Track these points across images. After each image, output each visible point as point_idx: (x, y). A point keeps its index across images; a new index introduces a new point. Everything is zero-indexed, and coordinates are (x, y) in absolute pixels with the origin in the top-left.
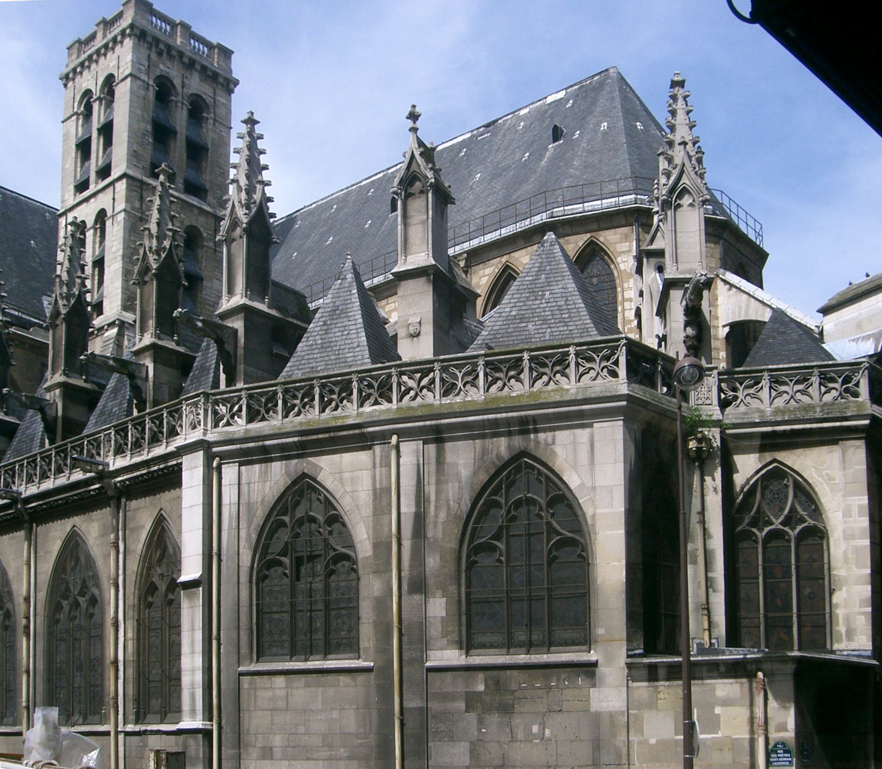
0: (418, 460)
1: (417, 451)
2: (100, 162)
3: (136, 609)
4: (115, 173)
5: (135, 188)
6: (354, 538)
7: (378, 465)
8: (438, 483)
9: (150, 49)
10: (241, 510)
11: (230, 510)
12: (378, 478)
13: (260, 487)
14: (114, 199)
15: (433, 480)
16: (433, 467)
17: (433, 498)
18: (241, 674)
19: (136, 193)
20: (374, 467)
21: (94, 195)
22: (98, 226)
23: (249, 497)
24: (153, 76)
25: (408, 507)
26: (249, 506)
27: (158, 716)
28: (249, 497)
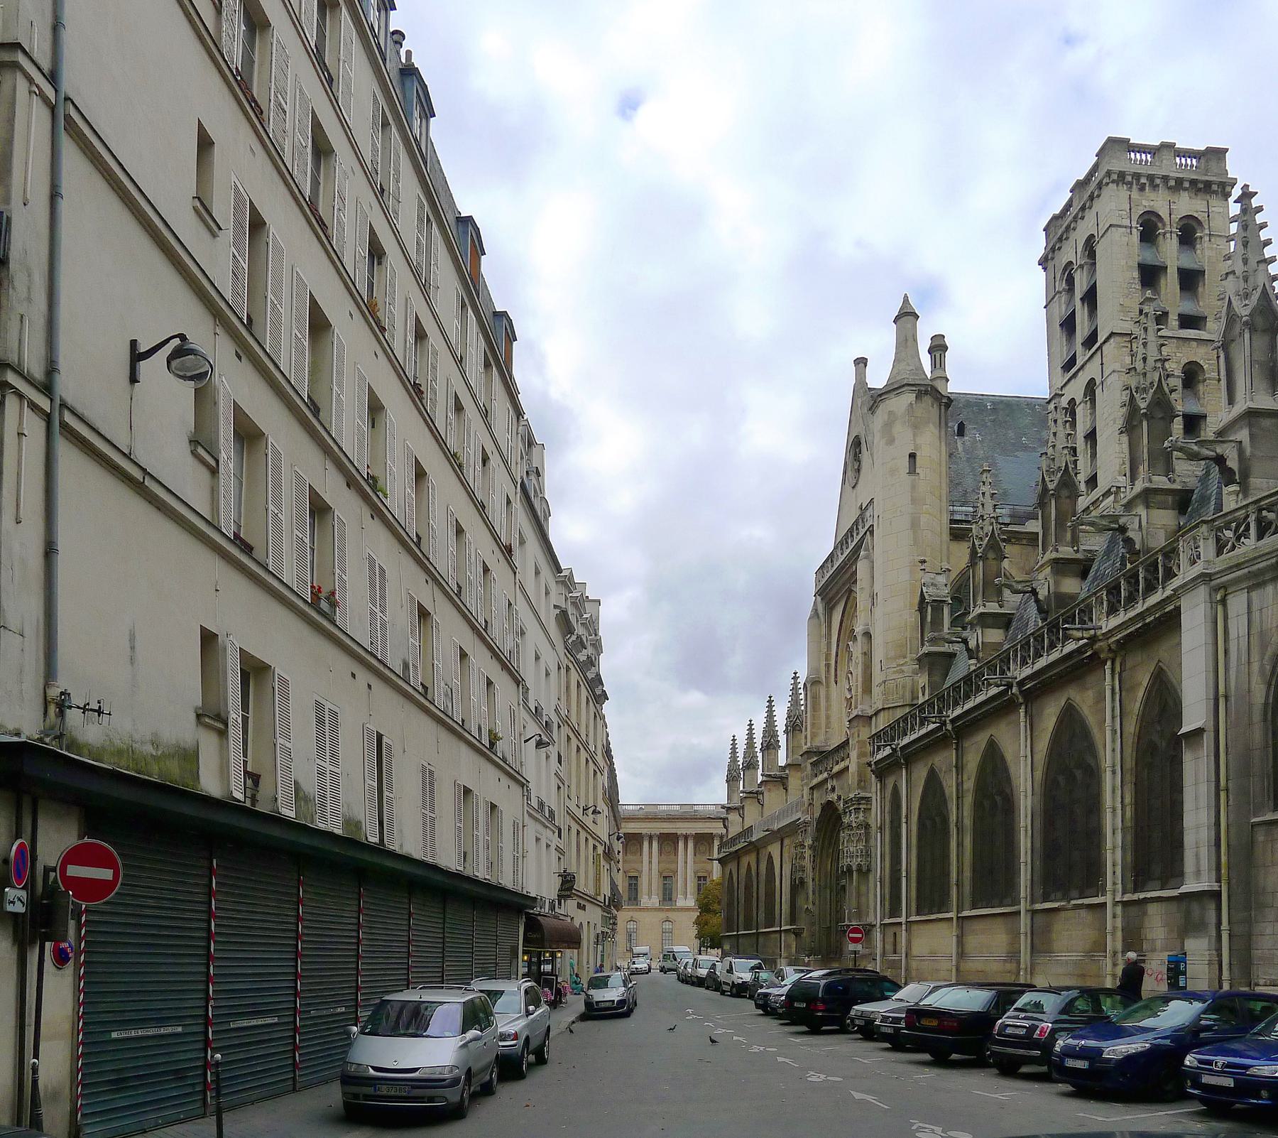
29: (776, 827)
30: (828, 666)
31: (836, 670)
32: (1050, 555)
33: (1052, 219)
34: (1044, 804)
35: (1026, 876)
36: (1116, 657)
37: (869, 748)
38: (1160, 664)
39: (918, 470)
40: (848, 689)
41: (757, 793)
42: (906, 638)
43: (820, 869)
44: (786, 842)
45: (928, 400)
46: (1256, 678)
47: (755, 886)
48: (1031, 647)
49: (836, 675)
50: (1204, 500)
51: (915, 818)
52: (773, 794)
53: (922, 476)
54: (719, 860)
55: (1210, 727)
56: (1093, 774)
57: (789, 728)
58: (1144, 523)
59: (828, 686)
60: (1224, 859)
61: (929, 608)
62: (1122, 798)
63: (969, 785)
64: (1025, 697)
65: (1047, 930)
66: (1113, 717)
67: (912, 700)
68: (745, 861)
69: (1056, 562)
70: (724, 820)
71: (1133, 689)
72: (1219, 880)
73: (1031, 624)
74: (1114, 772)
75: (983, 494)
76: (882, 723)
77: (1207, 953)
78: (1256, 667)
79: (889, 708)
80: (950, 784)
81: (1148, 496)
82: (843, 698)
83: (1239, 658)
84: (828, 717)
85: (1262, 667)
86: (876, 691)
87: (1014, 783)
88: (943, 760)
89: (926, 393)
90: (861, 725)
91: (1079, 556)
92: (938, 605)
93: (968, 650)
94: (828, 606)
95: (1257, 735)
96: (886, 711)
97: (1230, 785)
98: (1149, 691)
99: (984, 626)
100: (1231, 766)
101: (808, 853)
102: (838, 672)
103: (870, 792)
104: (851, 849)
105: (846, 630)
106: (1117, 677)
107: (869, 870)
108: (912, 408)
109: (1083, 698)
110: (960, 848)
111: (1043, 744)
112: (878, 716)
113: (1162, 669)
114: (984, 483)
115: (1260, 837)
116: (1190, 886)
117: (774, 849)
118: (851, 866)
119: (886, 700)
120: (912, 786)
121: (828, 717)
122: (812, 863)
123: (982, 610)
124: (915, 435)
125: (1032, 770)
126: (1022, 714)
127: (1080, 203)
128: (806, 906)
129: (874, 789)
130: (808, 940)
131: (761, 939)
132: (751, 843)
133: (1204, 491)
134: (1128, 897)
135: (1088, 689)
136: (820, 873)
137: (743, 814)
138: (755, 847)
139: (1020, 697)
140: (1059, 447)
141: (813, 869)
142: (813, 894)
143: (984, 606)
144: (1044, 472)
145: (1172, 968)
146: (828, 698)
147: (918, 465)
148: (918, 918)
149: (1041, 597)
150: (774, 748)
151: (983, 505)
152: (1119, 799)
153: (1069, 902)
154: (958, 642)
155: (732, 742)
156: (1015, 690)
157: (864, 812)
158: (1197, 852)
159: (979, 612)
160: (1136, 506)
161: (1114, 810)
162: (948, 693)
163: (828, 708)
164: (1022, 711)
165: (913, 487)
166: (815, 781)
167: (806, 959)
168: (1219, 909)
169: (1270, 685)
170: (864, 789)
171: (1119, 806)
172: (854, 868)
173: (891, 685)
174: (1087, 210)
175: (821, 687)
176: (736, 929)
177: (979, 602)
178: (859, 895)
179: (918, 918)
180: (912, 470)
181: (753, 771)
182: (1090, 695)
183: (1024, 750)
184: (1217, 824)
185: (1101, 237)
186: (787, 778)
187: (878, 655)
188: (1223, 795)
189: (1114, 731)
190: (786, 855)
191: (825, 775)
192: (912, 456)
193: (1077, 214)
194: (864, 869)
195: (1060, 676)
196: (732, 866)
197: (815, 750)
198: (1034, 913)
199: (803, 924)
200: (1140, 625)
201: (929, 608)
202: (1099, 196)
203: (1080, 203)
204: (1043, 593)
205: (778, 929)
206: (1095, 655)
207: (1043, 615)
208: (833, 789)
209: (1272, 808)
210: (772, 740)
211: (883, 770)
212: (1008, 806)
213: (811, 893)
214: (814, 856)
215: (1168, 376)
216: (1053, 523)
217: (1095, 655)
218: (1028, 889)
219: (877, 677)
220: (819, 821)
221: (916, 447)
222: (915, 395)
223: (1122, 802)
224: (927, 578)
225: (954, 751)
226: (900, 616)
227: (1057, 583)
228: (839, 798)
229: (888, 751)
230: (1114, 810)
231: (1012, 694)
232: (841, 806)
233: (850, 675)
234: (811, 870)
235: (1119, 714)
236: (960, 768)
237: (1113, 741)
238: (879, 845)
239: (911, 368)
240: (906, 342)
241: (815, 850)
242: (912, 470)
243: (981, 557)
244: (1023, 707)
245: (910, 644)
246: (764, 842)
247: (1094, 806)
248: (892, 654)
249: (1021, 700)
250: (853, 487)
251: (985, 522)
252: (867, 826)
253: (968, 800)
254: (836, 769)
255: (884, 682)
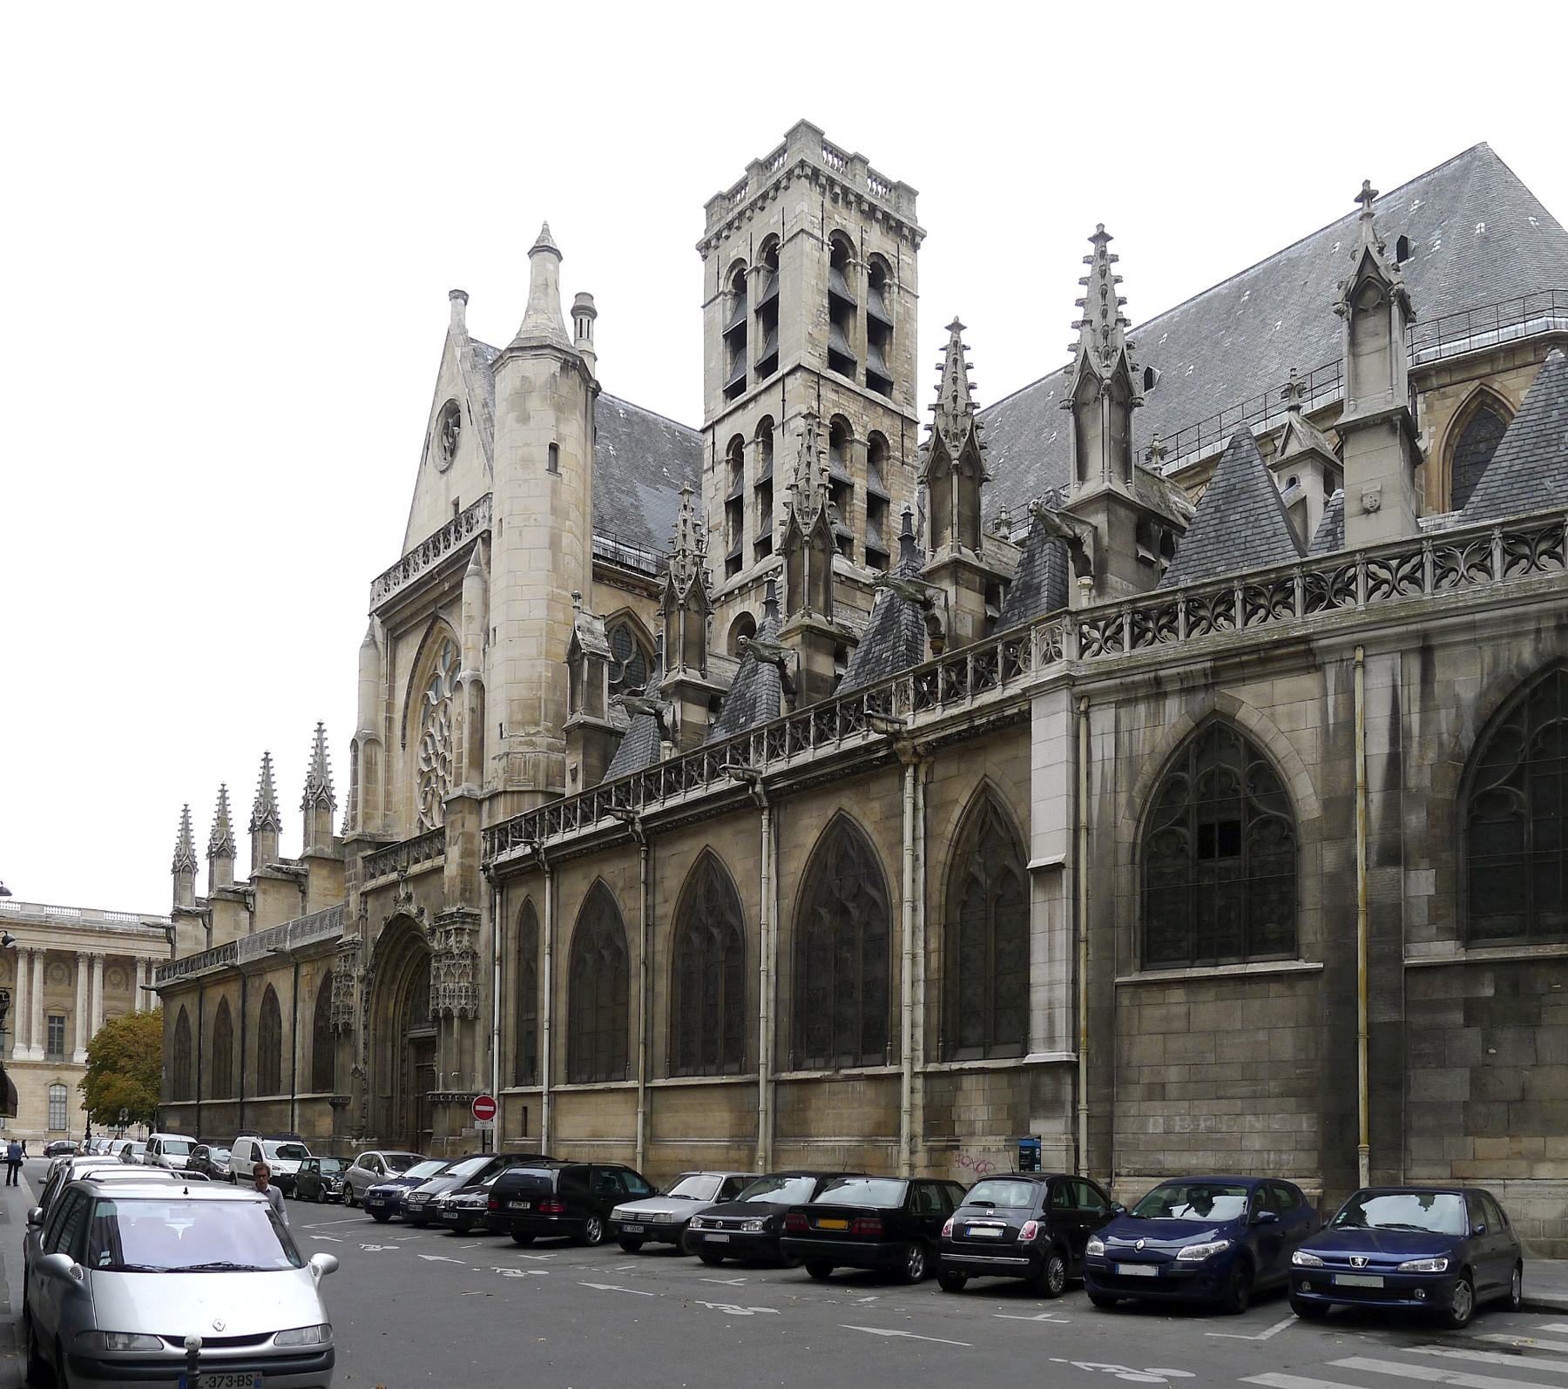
0: (1394, 680)
1: (1393, 669)
2: (760, 354)
3: (943, 911)
4: (784, 367)
5: (812, 384)
6: (1292, 794)
7: (1331, 691)
8: (1424, 710)
9: (823, 194)
10: (1119, 767)
11: (1103, 768)
12: (1331, 710)
13: (1148, 734)
14: (784, 400)
15: (1416, 708)
16: (1416, 689)
17: (1416, 730)
18: (1118, 986)
19: (812, 391)
20: (1325, 695)
21: (754, 398)
22: (760, 439)
23: (1131, 751)
24: (827, 232)
25: (1379, 746)
26: (1131, 761)
27: (981, 1049)
28: (1131, 751)
29: (288, 946)
30: (390, 720)
31: (404, 728)
32: (798, 619)
33: (716, 198)
34: (797, 943)
35: (767, 1036)
36: (920, 762)
37: (484, 846)
38: (987, 779)
39: (560, 470)
40: (424, 759)
41: (245, 894)
42: (540, 698)
43: (376, 1012)
44: (304, 970)
45: (575, 374)
46: (1122, 811)
47: (237, 1033)
48: (777, 738)
49: (404, 736)
50: (1030, 589)
51: (565, 949)
52: (270, 899)
53: (566, 477)
54: (160, 991)
55: (1069, 864)
56: (881, 913)
57: (311, 803)
58: (952, 601)
59: (389, 750)
60: (1083, 1023)
61: (586, 663)
62: (925, 942)
63: (667, 909)
64: (770, 800)
65: (802, 1106)
66: (914, 839)
67: (547, 785)
68: (215, 995)
69: (808, 630)
70: (168, 929)
71: (944, 806)
72: (1075, 1049)
73: (762, 707)
74: (914, 909)
75: (685, 521)
76: (502, 813)
77: (1063, 1137)
78: (1123, 798)
79: (513, 792)
80: (632, 907)
81: (955, 569)
82: (415, 772)
83: (1103, 786)
84: (388, 794)
85: (1130, 801)
86: (490, 765)
87: (748, 912)
88: (618, 873)
89: (574, 366)
90: (466, 811)
91: (833, 629)
92: (597, 659)
93: (661, 726)
94: (391, 636)
95: (1125, 879)
96: (509, 796)
97: (1090, 936)
98: (968, 813)
99: (684, 699)
100: (1091, 911)
101: (357, 989)
102: (408, 733)
103: (478, 908)
104: (448, 988)
105: (423, 672)
106: (920, 789)
107: (476, 1018)
108: (556, 381)
109: (866, 813)
110: (650, 993)
111: (797, 864)
112: (495, 802)
113: (989, 786)
114: (685, 507)
115: (1125, 1000)
116: (1038, 1056)
117: (282, 983)
118: (450, 1010)
119: (509, 780)
120: (560, 904)
121: (388, 794)
122: (364, 1004)
123: (681, 676)
124: (558, 420)
125: (777, 896)
126: (765, 823)
127: (759, 188)
128: (354, 1066)
129: (485, 903)
130: (357, 1114)
131: (249, 1112)
132: (233, 967)
133: (1028, 578)
134: (932, 1067)
135: (872, 800)
136: (375, 1019)
137: (211, 925)
138: (241, 975)
139: (764, 799)
140: (814, 483)
141: (366, 1011)
142: (365, 1048)
143: (685, 671)
144: (795, 511)
145: (1026, 1155)
146: (389, 767)
147: (560, 463)
148: (570, 1087)
149: (789, 672)
150: (273, 830)
151: (684, 536)
152: (921, 944)
153: (837, 1071)
154: (651, 714)
155: (182, 814)
156: (758, 788)
157: (469, 935)
158: (1049, 1014)
159: (678, 678)
160: (940, 579)
161: (914, 957)
162: (637, 782)
163: (388, 781)
164: (765, 818)
165: (555, 492)
166: (371, 884)
167: (354, 1143)
168: (1076, 1085)
169: (1139, 821)
170: (469, 901)
171: (921, 952)
172: (456, 1013)
173: (518, 760)
174: (769, 200)
175: (378, 749)
176: (194, 1093)
177: (678, 663)
178: (461, 1052)
179: (570, 1087)
180: (553, 468)
181: (227, 860)
182: (876, 807)
183: (768, 869)
184: (1075, 982)
185: (788, 241)
186: (306, 876)
187: (496, 714)
188: (1083, 946)
189: (915, 858)
190: (304, 991)
191: (394, 876)
192: (554, 448)
193: (755, 201)
194: (470, 1016)
195: (831, 778)
196: (190, 1002)
197: (369, 839)
198: (778, 1084)
199: (345, 1088)
200: (965, 727)
201: (586, 663)
202: (786, 188)
203: (759, 188)
204: (791, 667)
205: (290, 1097)
206: (892, 758)
207: (790, 696)
208: (409, 898)
209: (1139, 966)
210: (270, 818)
211: (503, 879)
212: (736, 945)
213: (361, 1046)
214: (368, 993)
215: (977, 427)
216: (806, 578)
217: (892, 758)
218: (770, 1054)
219: (493, 745)
220: (378, 945)
221: (559, 434)
222: (559, 364)
223: (925, 948)
224: (581, 620)
225: (643, 862)
226: (533, 666)
227: (808, 658)
228: (421, 912)
229: (521, 851)
230: (914, 957)
231: (754, 793)
232: (426, 923)
233: (428, 739)
234: (363, 1013)
235: (922, 835)
236: (651, 885)
237: (914, 869)
238: (498, 986)
239: (552, 325)
240: (544, 287)
241: (369, 984)
242: (553, 468)
243: (682, 605)
244: (766, 812)
245: (546, 706)
246: (258, 968)
247: (881, 947)
248: (518, 717)
249: (765, 804)
250: (442, 472)
251: (687, 560)
252: (475, 956)
253: (665, 929)
254: (415, 869)
255: (507, 754)
